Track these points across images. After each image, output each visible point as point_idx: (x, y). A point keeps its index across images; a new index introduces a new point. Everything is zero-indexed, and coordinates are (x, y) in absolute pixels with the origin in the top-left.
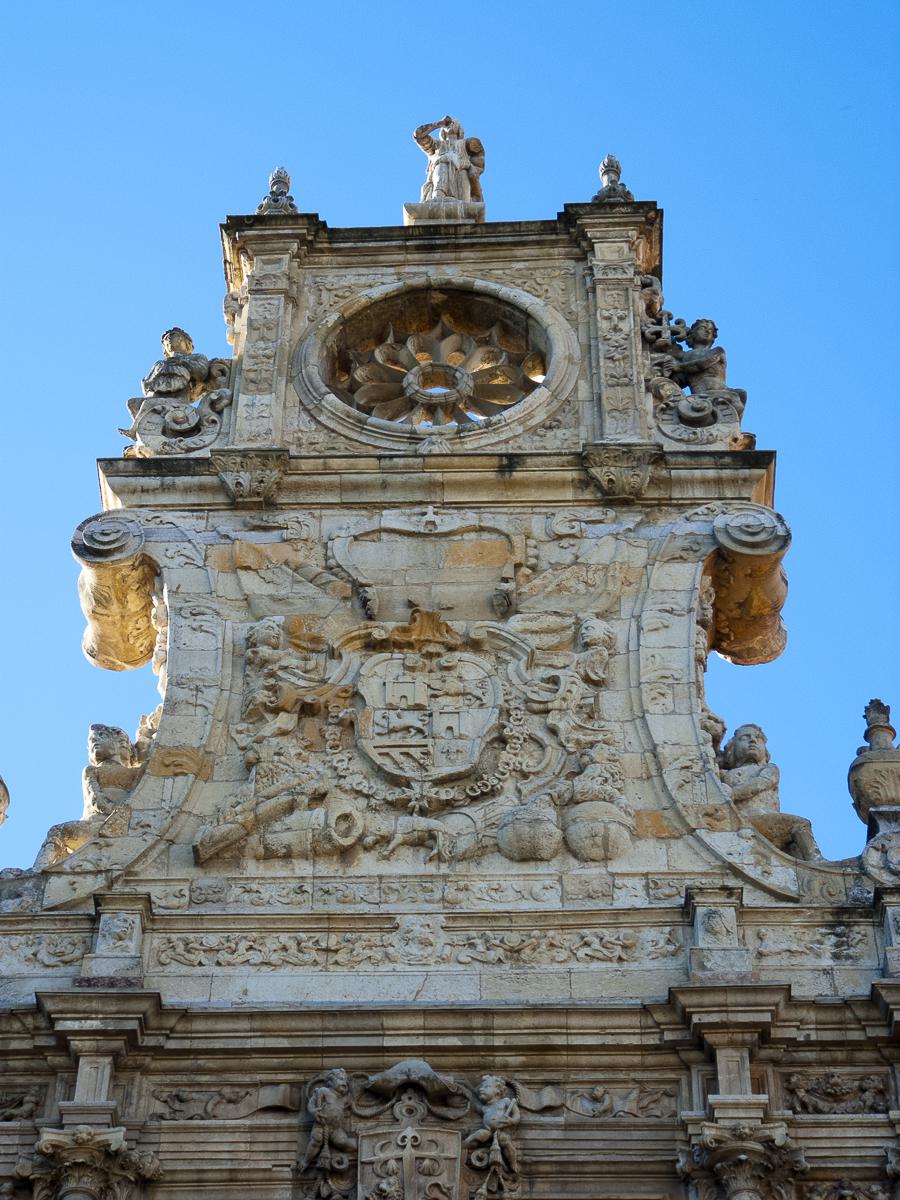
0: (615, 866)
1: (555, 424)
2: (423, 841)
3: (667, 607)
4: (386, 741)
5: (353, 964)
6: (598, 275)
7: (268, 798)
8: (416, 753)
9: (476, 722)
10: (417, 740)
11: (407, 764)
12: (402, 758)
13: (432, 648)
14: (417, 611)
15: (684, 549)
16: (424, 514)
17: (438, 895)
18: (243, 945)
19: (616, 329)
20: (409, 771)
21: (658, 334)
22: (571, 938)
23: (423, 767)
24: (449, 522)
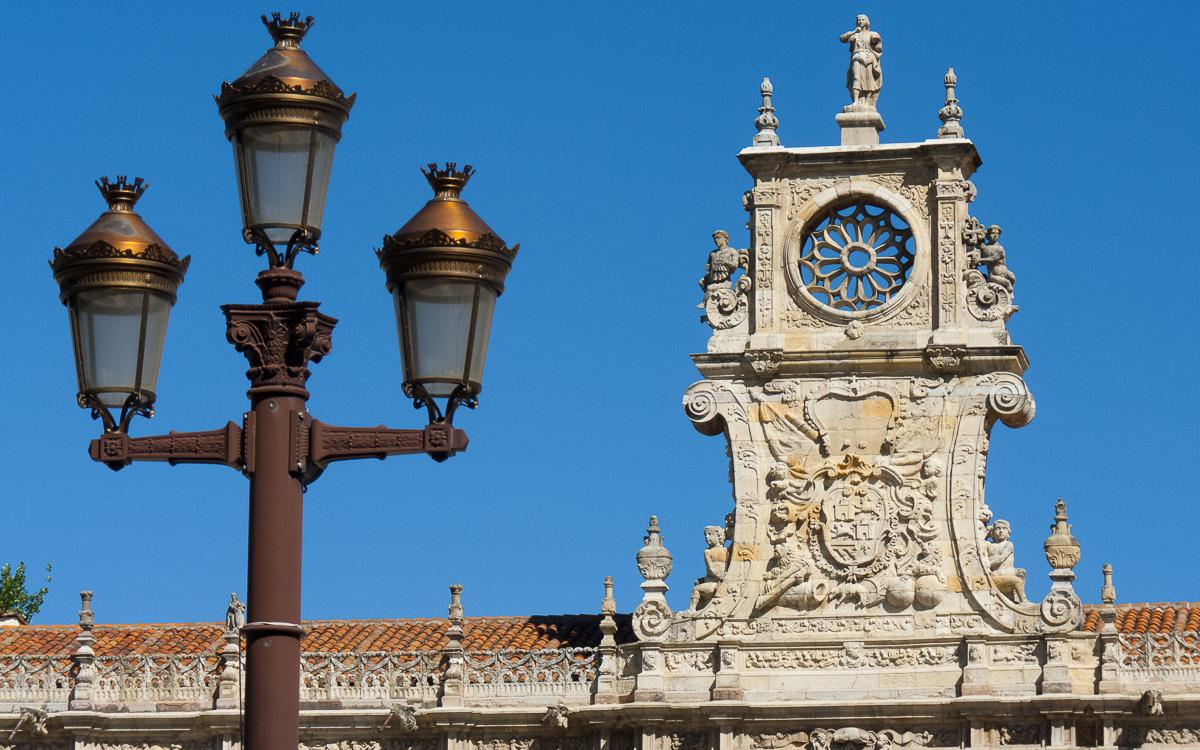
0: (938, 609)
1: (916, 304)
2: (854, 598)
3: (965, 448)
4: (835, 542)
5: (827, 666)
6: (940, 195)
7: (786, 578)
8: (850, 551)
9: (876, 529)
10: (849, 542)
11: (847, 557)
12: (843, 553)
13: (857, 478)
14: (847, 456)
15: (976, 407)
16: (850, 382)
17: (862, 627)
18: (781, 657)
19: (947, 237)
20: (849, 561)
21: (970, 236)
22: (914, 653)
23: (853, 557)
24: (864, 385)
